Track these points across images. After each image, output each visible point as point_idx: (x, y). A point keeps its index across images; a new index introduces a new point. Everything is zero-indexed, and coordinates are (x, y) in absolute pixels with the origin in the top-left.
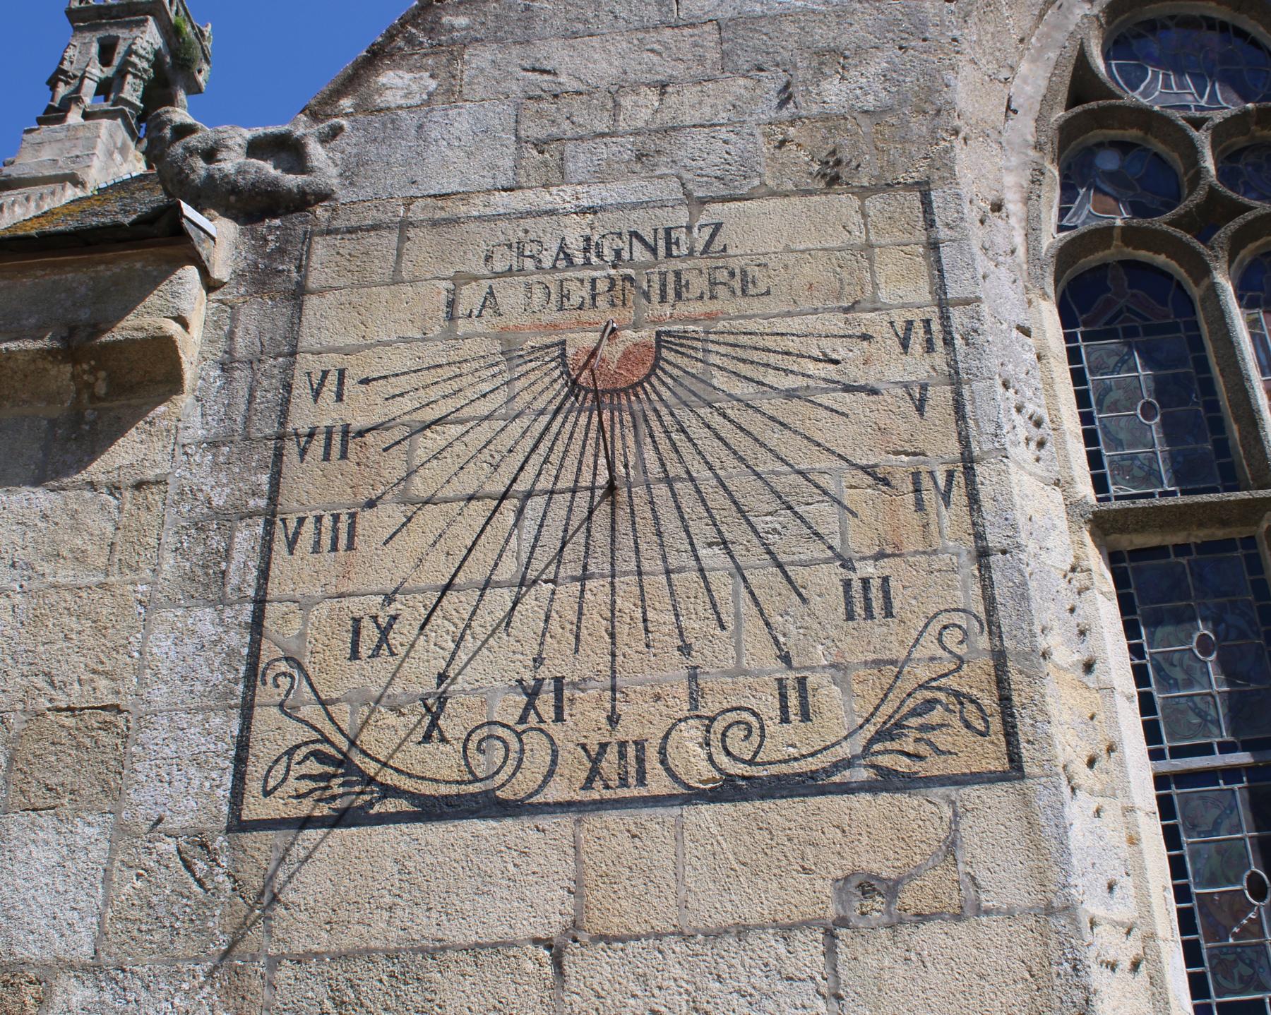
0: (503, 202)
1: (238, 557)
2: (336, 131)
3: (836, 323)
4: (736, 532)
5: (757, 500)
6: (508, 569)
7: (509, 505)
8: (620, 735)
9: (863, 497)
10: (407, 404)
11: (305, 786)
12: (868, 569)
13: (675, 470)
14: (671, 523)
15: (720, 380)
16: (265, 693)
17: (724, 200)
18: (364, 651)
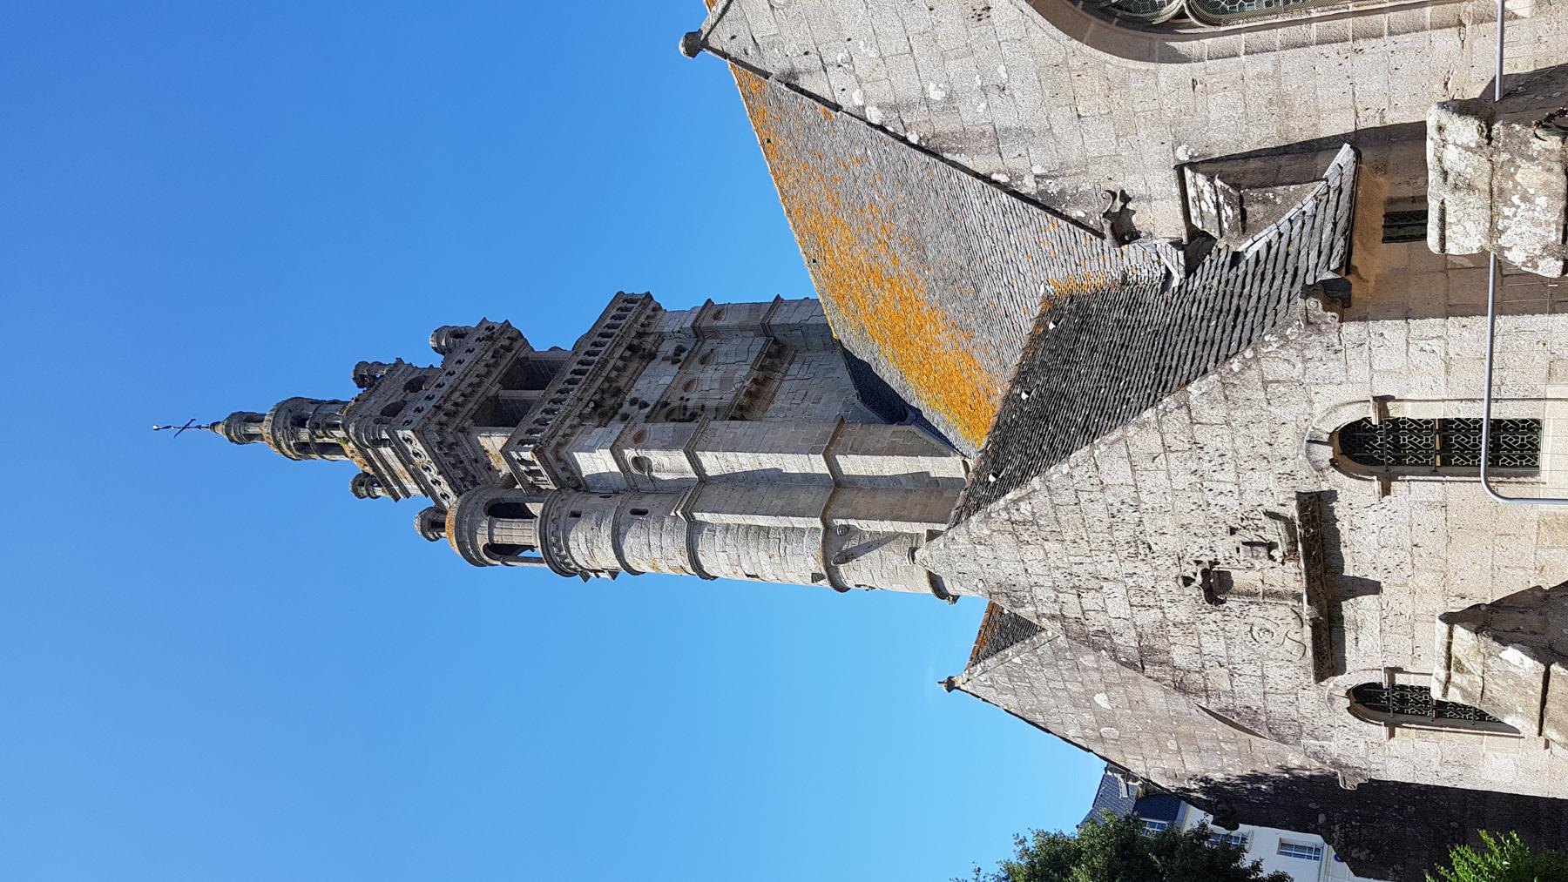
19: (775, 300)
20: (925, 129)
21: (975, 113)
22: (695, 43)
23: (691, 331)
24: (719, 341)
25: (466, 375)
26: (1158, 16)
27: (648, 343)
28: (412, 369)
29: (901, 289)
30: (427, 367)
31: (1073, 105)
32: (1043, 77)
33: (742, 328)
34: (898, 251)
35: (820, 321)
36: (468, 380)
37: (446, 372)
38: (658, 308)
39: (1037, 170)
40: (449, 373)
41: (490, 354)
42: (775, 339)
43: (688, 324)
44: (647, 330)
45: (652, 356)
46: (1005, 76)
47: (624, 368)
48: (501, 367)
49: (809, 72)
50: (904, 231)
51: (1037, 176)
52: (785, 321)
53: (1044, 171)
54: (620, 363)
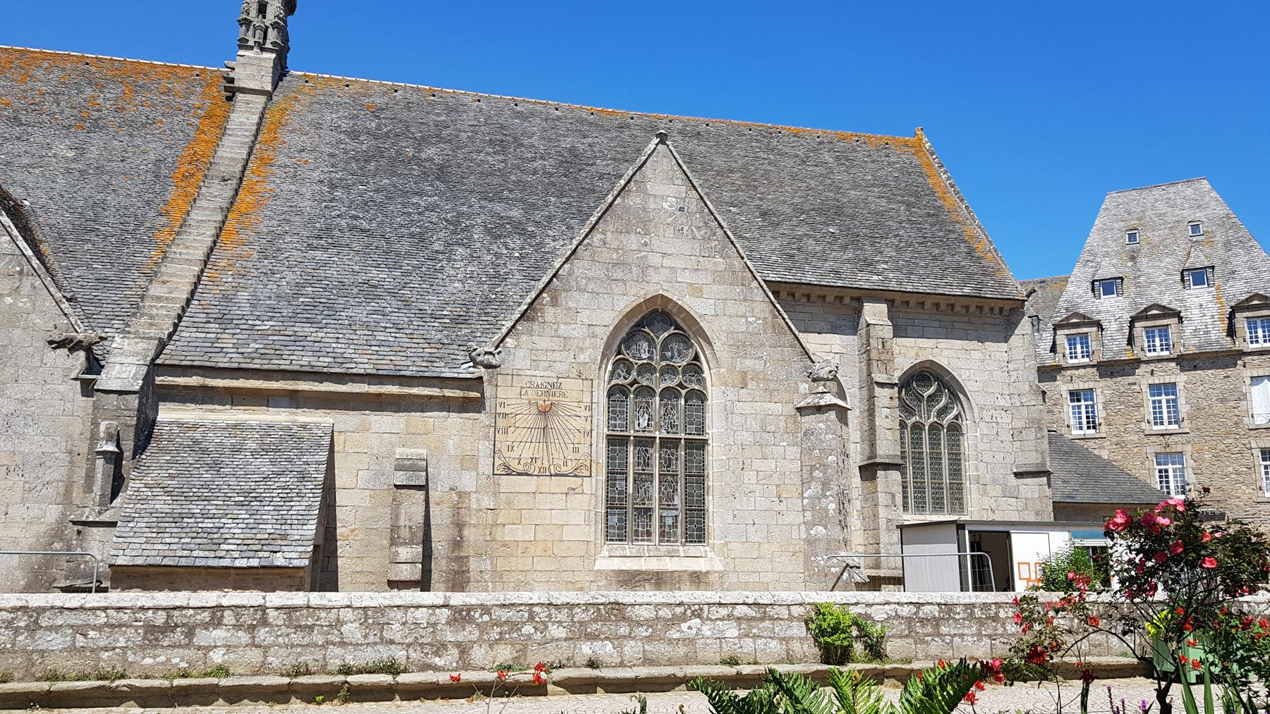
0: (528, 373)
2: (500, 352)
3: (576, 404)
4: (560, 438)
5: (563, 433)
6: (529, 440)
9: (577, 434)
10: (514, 410)
12: (576, 446)
16: (496, 455)
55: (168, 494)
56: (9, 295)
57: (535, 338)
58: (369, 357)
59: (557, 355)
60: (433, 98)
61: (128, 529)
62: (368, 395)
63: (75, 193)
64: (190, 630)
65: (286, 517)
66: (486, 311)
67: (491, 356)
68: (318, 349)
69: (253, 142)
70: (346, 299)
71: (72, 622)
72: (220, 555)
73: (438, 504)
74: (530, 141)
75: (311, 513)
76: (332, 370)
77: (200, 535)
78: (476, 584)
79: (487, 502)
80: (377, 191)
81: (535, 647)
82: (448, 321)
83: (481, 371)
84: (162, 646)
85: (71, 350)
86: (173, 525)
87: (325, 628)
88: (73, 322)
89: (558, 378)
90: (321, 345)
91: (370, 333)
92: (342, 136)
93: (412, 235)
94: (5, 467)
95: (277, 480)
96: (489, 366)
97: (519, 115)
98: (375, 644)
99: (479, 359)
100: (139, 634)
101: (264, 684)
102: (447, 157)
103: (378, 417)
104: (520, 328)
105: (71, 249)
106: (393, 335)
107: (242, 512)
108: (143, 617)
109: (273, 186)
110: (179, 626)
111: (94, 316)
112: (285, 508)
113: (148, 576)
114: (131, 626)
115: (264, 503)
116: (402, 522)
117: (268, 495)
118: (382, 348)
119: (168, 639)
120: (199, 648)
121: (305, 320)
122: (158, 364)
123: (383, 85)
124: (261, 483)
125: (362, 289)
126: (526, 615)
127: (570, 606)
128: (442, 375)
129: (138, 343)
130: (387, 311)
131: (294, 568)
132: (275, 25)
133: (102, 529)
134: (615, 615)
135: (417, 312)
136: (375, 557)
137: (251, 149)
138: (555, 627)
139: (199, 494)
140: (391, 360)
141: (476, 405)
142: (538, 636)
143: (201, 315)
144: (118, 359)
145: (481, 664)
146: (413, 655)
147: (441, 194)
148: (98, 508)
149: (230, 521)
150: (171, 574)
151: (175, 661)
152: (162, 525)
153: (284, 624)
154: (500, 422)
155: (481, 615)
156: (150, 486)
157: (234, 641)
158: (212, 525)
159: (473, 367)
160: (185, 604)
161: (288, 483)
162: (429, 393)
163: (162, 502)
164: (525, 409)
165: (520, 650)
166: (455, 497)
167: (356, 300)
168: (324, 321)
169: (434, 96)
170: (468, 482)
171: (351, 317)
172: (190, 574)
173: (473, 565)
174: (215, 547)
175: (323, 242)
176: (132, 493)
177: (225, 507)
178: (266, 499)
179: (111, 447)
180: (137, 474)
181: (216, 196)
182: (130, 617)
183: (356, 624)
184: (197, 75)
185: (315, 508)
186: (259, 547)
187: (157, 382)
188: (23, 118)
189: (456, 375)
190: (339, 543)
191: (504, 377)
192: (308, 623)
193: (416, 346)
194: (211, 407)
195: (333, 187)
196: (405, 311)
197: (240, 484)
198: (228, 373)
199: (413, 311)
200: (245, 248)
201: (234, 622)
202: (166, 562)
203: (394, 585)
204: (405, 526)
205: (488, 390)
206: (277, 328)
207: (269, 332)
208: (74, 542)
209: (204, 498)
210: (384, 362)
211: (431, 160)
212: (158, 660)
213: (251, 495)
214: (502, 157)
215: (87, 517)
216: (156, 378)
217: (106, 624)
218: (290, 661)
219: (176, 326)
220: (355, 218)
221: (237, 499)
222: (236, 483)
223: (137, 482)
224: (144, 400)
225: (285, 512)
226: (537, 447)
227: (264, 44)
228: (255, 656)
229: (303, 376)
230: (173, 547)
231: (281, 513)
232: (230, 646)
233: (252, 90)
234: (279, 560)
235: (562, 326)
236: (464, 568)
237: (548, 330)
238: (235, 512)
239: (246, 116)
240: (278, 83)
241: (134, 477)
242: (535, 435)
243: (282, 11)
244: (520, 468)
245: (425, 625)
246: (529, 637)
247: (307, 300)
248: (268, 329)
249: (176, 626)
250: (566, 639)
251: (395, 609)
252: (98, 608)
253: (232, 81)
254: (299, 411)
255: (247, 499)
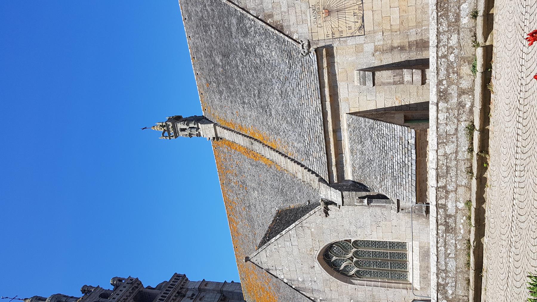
0: (309, 24)
1: (343, 40)
2: (301, 41)
6: (345, 18)
7: (339, 19)
8: (358, 8)
11: (361, 30)
13: (336, 7)
14: (341, 7)
15: (328, 4)
16: (354, 35)
17: (309, 5)
18: (351, 28)
19: (225, 282)
20: (297, 286)
21: (308, 285)
22: (247, 259)
23: (198, 289)
24: (206, 293)
25: (123, 296)
26: (348, 274)
27: (183, 291)
28: (102, 290)
29: (270, 295)
30: (108, 289)
31: (330, 287)
32: (324, 281)
33: (213, 290)
34: (271, 286)
35: (239, 291)
36: (123, 298)
37: (116, 294)
38: (187, 280)
39: (321, 298)
40: (117, 294)
41: (131, 289)
42: (223, 295)
43: (197, 287)
44: (184, 287)
45: (184, 296)
46: (316, 279)
47: (175, 300)
48: (134, 294)
49: (272, 270)
50: (274, 282)
51: (320, 300)
52: (227, 290)
53: (322, 299)
54: (174, 298)
55: (383, 180)
56: (311, 230)
57: (291, 23)
58: (313, 100)
59: (298, 9)
60: (195, 58)
61: (400, 196)
62: (331, 101)
63: (270, 193)
64: (448, 216)
65: (391, 137)
66: (283, 42)
67: (304, 45)
68: (313, 121)
69: (235, 132)
70: (290, 105)
71: (443, 259)
72: (411, 164)
73: (382, 61)
74: (199, 12)
75: (389, 126)
76: (322, 118)
77: (402, 171)
78: (423, 36)
79: (379, 36)
80: (241, 85)
81: (462, 52)
82: (291, 61)
83: (312, 49)
84: (455, 226)
85: (328, 210)
86: (397, 180)
87: (448, 161)
88: (317, 210)
89: (310, 7)
90: (311, 119)
91: (303, 97)
92: (222, 97)
93: (256, 72)
94: (377, 227)
95: (374, 139)
96: (309, 46)
97: (190, 16)
98: (457, 137)
99: (306, 51)
100: (449, 235)
101: (476, 190)
102: (218, 53)
103: (341, 94)
104: (287, 32)
105: (290, 198)
106: (302, 88)
107: (390, 154)
108: (441, 234)
109: (250, 126)
110: (446, 221)
111: (314, 195)
112: (387, 137)
113: (421, 190)
114: (445, 238)
115: (385, 145)
116: (392, 81)
117: (381, 143)
118: (309, 93)
119: (452, 225)
120: (456, 212)
121: (302, 123)
122: (329, 182)
123: (197, 79)
124: (376, 145)
125: (284, 97)
126: (443, 60)
127: (438, 33)
128: (317, 69)
129: (322, 189)
130: (292, 88)
131: (416, 136)
132: (187, 125)
133: (400, 202)
134: (445, 4)
135: (289, 75)
136: (410, 87)
137: (237, 133)
138: (451, 42)
139: (383, 169)
140: (313, 91)
141: (330, 50)
142: (456, 51)
143: (307, 162)
144: (330, 197)
145: (471, 82)
146: (464, 118)
147: (235, 57)
148: (391, 204)
149: (394, 159)
150: (419, 181)
151: (462, 221)
152: (397, 184)
153: (446, 179)
154: (337, 35)
155: (443, 85)
156: (381, 186)
157: (454, 199)
158: (397, 167)
159: (311, 53)
160: (435, 219)
161: (375, 134)
162: (327, 74)
163: (387, 183)
164: (328, 23)
165: (464, 61)
166: (378, 53)
167: (289, 100)
168: (301, 115)
169: (194, 58)
170: (369, 48)
171: (297, 104)
172: (419, 174)
173: (413, 39)
174: (407, 166)
175: (268, 110)
176: (384, 193)
177: (388, 160)
178: (383, 144)
179: (366, 201)
180: (376, 190)
181: (259, 148)
182: (441, 239)
183: (446, 147)
184: (216, 148)
185: (386, 125)
186: (406, 149)
187: (337, 182)
188: (247, 205)
189: (316, 63)
190: (403, 104)
191: (314, 37)
192: (445, 168)
193: (305, 78)
194: (344, 161)
195: (244, 103)
196: (290, 80)
197: (377, 153)
198: (329, 157)
199: (290, 76)
200: (277, 140)
201: (444, 200)
202: (414, 184)
203: (423, 82)
204: (393, 79)
205: (322, 44)
206: (307, 135)
207: (309, 138)
208: (407, 211)
209: (384, 167)
210: (315, 94)
211: (221, 60)
212: (461, 228)
213: (382, 149)
214: (210, 26)
215: (395, 207)
216: (335, 182)
217: (445, 247)
218: (464, 175)
219: (313, 172)
220: (254, 95)
221: (384, 155)
222: (377, 155)
223: (379, 190)
224: (345, 187)
225: (389, 137)
226: (348, 14)
227: (196, 128)
228: (461, 190)
229: (326, 129)
230: (407, 181)
231: (389, 138)
232: (456, 201)
233: (215, 131)
234: (413, 141)
235: (282, 9)
236: (415, 43)
237: (286, 17)
238: (390, 156)
239: (225, 134)
240: (209, 121)
241: (377, 191)
242: (341, 16)
243: (181, 123)
244: (360, 21)
245: (447, 114)
246: (456, 56)
247: (293, 121)
248: (308, 138)
249: (446, 221)
250: (459, 34)
251: (438, 129)
252: (437, 250)
253: (214, 138)
254: (342, 128)
255: (384, 151)
